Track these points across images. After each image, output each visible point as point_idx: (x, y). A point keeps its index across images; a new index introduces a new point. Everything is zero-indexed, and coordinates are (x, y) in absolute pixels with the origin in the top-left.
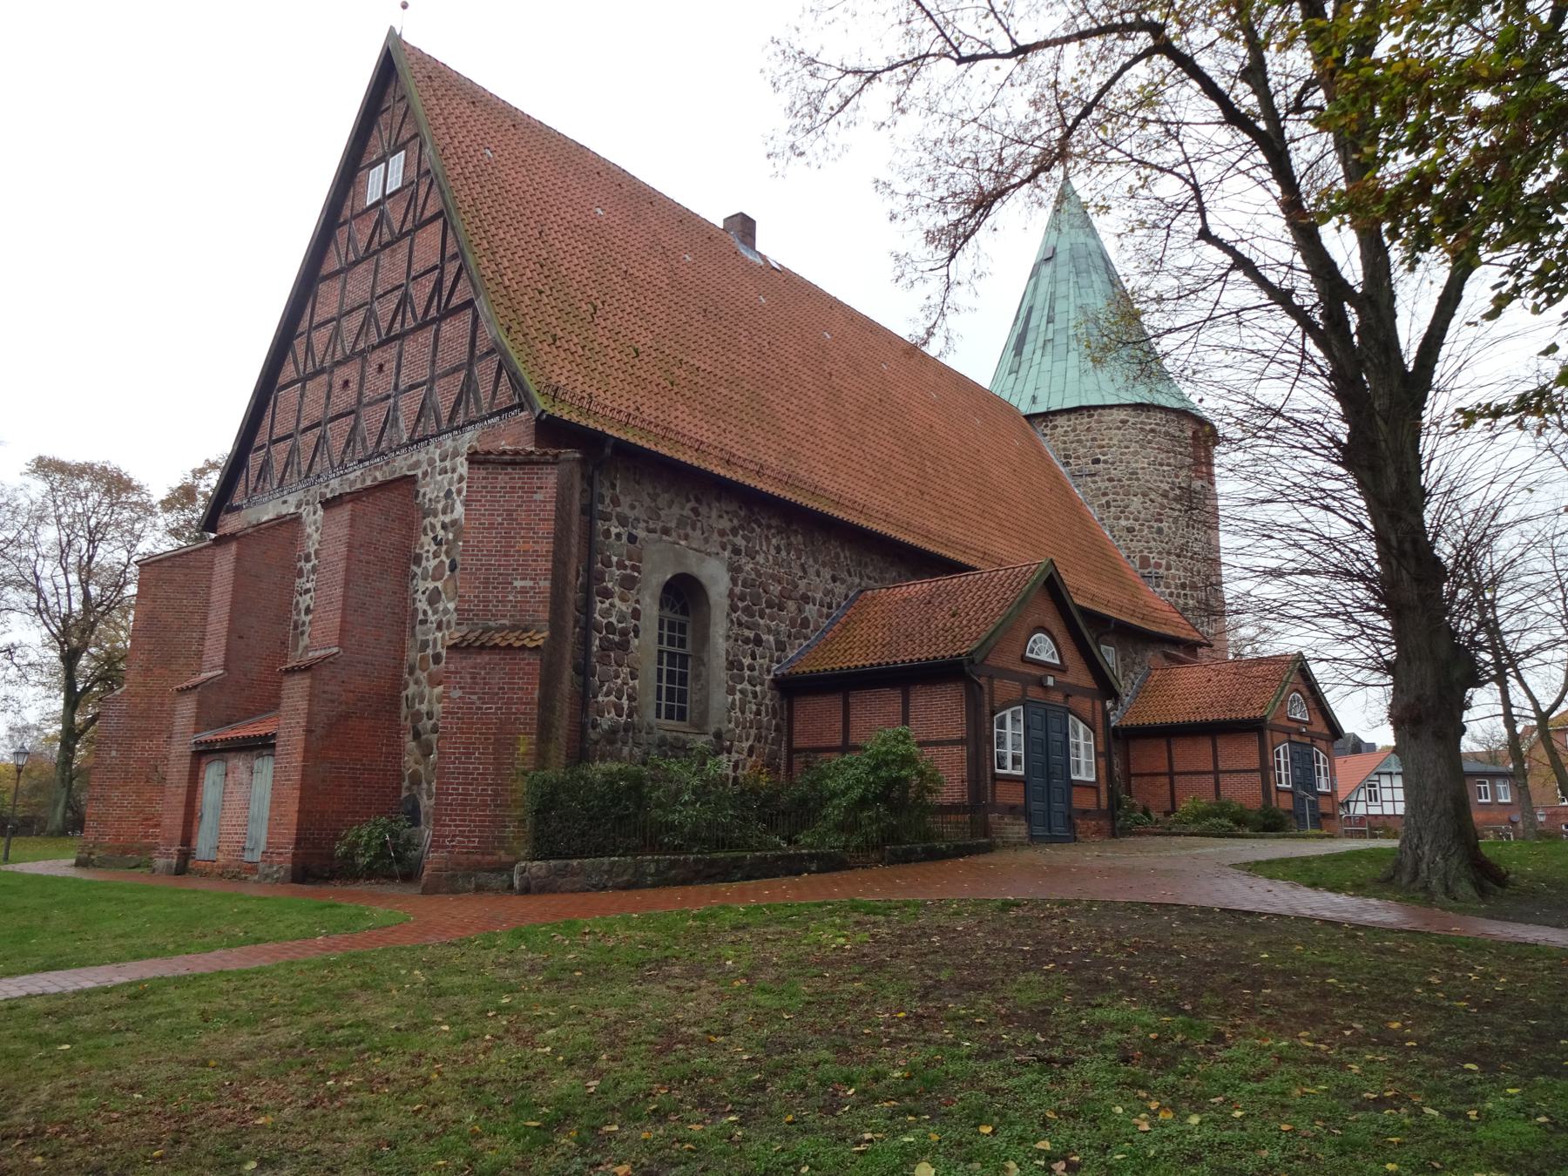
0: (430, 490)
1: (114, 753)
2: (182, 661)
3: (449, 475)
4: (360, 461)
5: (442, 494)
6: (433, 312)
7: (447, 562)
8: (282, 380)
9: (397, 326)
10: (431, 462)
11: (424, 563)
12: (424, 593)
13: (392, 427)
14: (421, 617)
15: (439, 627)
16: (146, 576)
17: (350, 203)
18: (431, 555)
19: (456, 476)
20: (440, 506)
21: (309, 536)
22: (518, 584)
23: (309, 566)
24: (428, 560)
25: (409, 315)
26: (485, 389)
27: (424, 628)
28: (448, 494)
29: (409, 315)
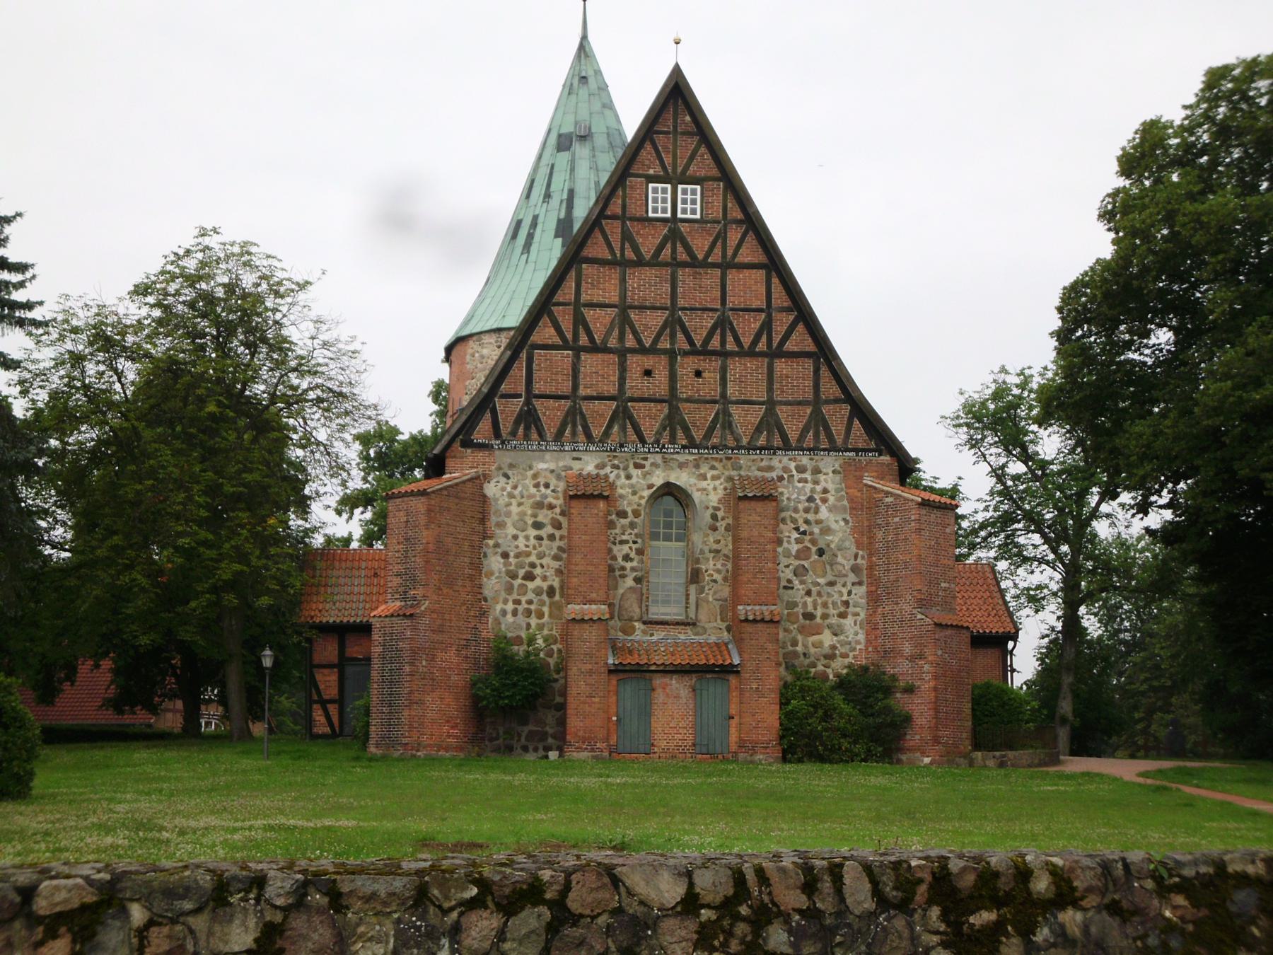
0: (792, 493)
1: (424, 663)
2: (460, 583)
3: (809, 486)
4: (684, 447)
5: (803, 498)
6: (762, 346)
7: (814, 549)
8: (535, 338)
9: (715, 343)
10: (786, 469)
11: (785, 545)
12: (787, 566)
13: (723, 427)
14: (784, 583)
15: (809, 593)
16: (433, 502)
17: (620, 202)
18: (793, 540)
19: (819, 488)
20: (801, 507)
21: (621, 496)
22: (943, 585)
23: (623, 521)
24: (789, 542)
25: (730, 339)
26: (837, 428)
27: (790, 592)
28: (810, 499)
29: (730, 339)
